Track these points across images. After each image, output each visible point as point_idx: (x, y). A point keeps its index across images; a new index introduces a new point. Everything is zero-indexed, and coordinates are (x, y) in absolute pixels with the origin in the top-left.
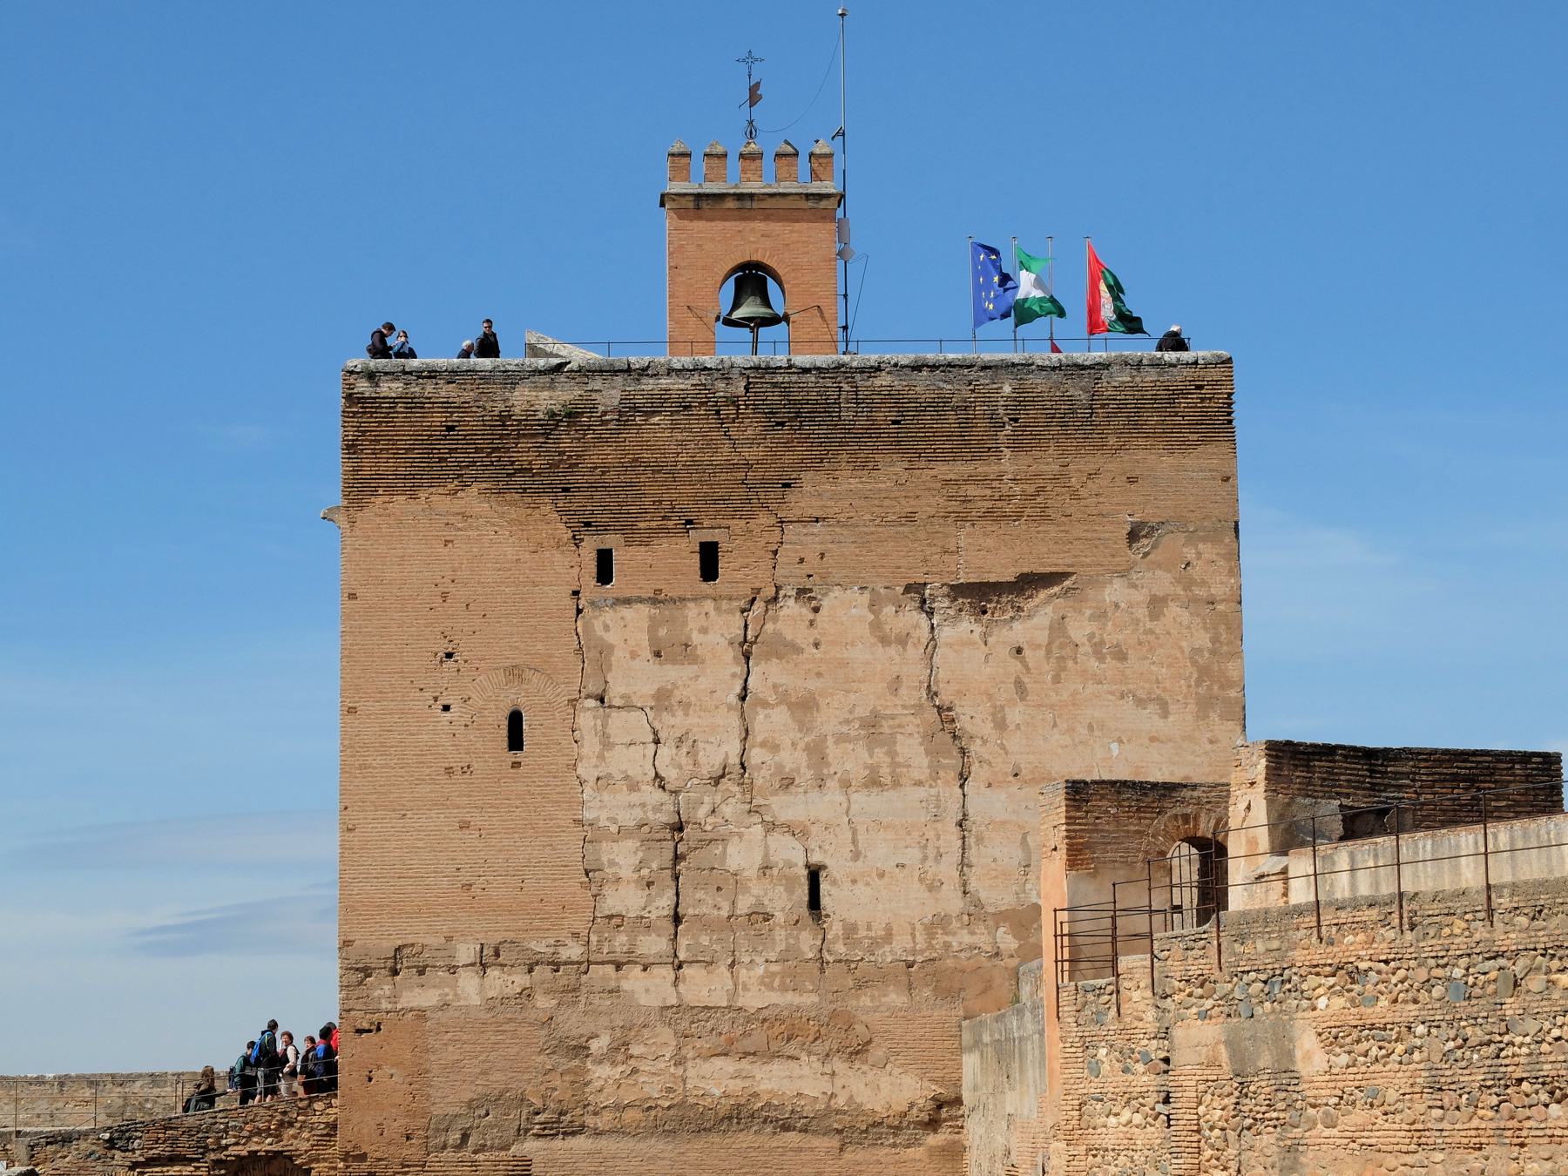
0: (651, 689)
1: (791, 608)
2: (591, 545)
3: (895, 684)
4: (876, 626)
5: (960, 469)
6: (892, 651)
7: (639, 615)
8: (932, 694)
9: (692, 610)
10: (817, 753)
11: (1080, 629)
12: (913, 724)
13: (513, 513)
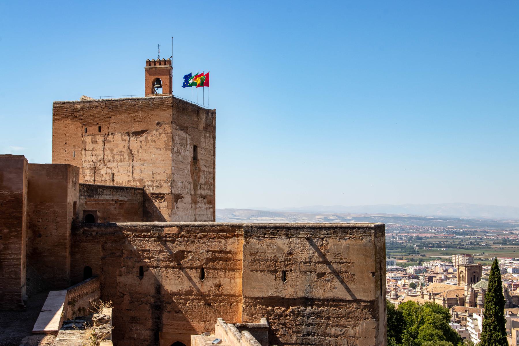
0: (91, 148)
1: (110, 136)
2: (84, 128)
3: (124, 147)
4: (122, 138)
5: (134, 114)
6: (124, 142)
7: (90, 137)
8: (129, 148)
9: (97, 137)
10: (113, 157)
11: (149, 138)
12: (126, 152)
13: (74, 123)
